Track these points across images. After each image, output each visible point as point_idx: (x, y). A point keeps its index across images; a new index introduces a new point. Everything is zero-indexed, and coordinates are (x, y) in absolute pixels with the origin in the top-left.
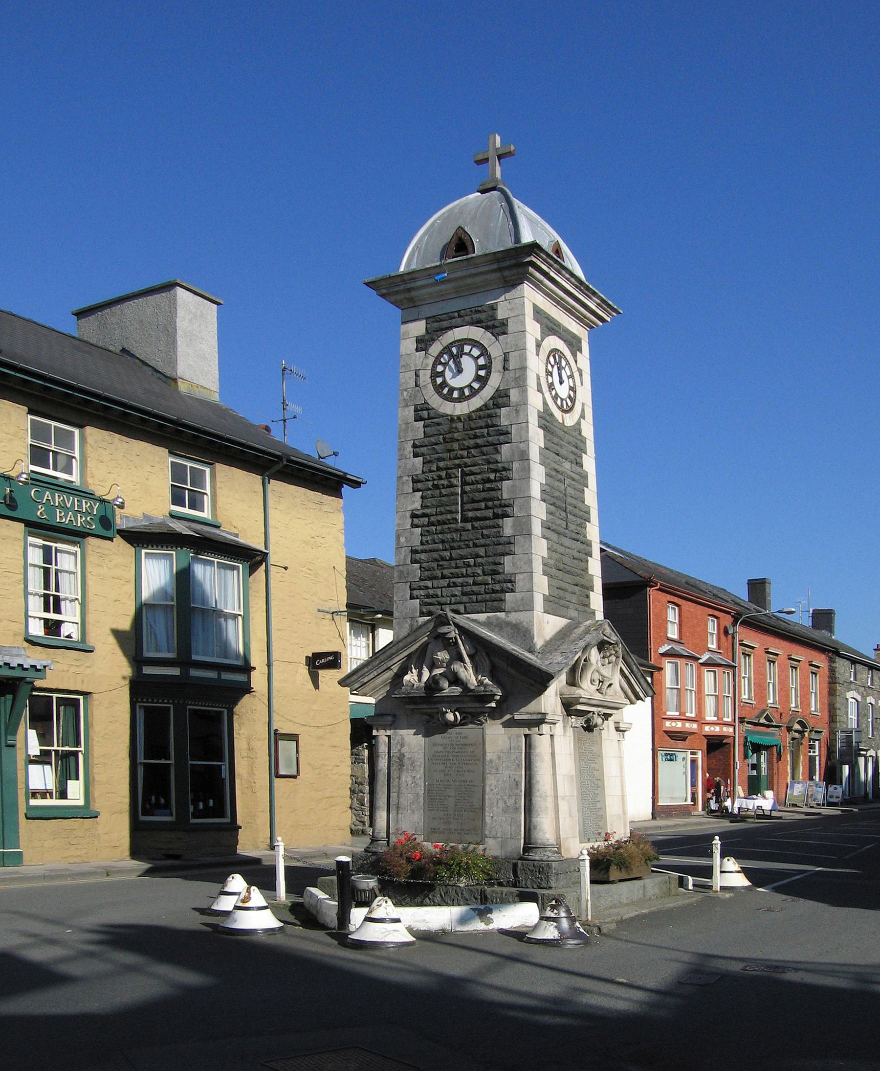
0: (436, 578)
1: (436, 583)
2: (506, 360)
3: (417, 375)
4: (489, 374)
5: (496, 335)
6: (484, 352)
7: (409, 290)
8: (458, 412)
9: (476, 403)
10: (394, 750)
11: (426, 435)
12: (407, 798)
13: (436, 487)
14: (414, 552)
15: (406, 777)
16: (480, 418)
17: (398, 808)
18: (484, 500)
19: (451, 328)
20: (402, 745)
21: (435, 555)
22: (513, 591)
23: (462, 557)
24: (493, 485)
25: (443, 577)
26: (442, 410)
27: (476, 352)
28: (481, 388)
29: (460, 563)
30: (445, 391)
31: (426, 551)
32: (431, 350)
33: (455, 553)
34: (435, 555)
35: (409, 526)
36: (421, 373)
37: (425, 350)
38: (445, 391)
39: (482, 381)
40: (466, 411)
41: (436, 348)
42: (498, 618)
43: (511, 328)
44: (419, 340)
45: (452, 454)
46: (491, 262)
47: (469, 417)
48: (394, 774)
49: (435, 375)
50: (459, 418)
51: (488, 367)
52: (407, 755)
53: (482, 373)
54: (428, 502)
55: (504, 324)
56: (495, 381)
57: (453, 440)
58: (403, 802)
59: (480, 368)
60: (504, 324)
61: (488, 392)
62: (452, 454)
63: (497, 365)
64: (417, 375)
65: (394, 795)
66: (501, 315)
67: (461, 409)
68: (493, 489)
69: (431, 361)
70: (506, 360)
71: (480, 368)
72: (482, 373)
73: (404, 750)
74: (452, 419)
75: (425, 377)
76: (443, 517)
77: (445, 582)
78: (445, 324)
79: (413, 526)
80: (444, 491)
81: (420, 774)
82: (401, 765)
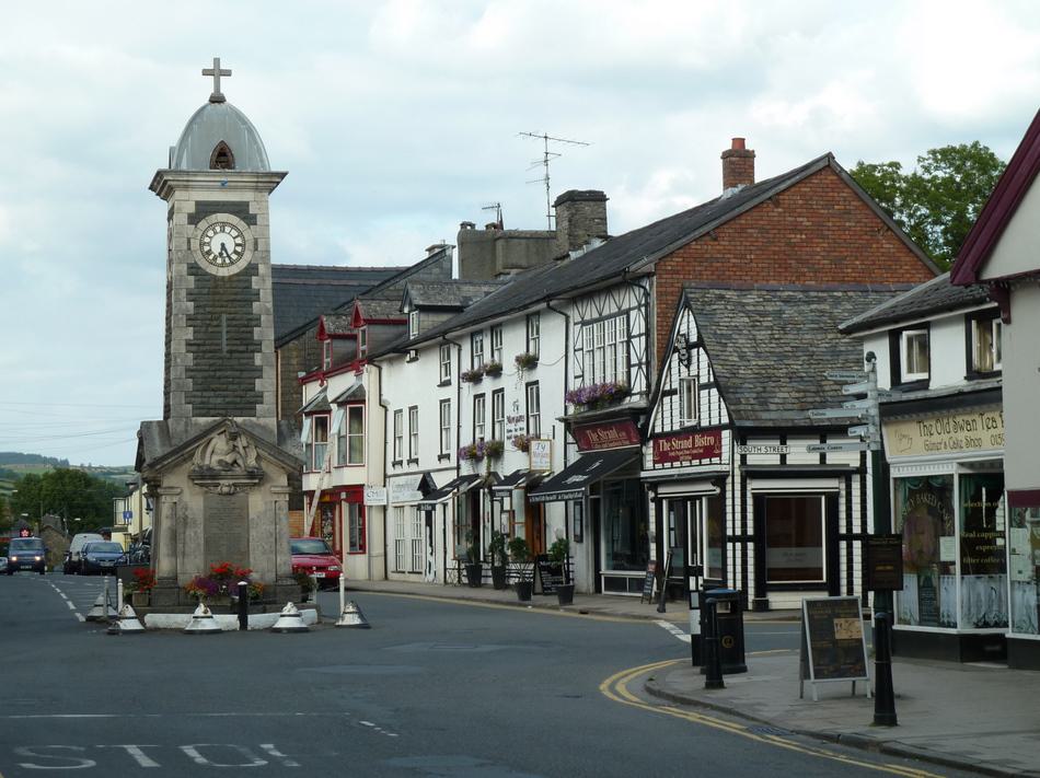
0: (205, 390)
1: (205, 394)
2: (256, 244)
3: (189, 242)
4: (244, 250)
6: (241, 234)
7: (188, 181)
8: (220, 274)
9: (234, 270)
10: (180, 513)
12: (191, 546)
15: (190, 532)
16: (239, 281)
17: (184, 554)
19: (215, 212)
20: (186, 509)
21: (206, 374)
22: (262, 403)
23: (227, 377)
24: (249, 329)
26: (208, 270)
27: (234, 233)
28: (238, 260)
29: (222, 380)
30: (211, 257)
32: (199, 225)
33: (218, 374)
34: (206, 374)
35: (184, 351)
36: (192, 241)
37: (196, 225)
38: (211, 257)
40: (227, 275)
41: (203, 225)
42: (251, 421)
47: (230, 277)
48: (180, 530)
49: (202, 244)
50: (223, 277)
52: (190, 517)
54: (199, 336)
55: (255, 216)
57: (218, 293)
59: (237, 245)
60: (255, 216)
61: (242, 264)
64: (189, 242)
65: (180, 546)
67: (223, 272)
69: (200, 233)
70: (256, 244)
71: (237, 245)
72: (239, 249)
74: (215, 277)
76: (213, 347)
77: (212, 394)
79: (188, 352)
81: (200, 530)
82: (185, 524)
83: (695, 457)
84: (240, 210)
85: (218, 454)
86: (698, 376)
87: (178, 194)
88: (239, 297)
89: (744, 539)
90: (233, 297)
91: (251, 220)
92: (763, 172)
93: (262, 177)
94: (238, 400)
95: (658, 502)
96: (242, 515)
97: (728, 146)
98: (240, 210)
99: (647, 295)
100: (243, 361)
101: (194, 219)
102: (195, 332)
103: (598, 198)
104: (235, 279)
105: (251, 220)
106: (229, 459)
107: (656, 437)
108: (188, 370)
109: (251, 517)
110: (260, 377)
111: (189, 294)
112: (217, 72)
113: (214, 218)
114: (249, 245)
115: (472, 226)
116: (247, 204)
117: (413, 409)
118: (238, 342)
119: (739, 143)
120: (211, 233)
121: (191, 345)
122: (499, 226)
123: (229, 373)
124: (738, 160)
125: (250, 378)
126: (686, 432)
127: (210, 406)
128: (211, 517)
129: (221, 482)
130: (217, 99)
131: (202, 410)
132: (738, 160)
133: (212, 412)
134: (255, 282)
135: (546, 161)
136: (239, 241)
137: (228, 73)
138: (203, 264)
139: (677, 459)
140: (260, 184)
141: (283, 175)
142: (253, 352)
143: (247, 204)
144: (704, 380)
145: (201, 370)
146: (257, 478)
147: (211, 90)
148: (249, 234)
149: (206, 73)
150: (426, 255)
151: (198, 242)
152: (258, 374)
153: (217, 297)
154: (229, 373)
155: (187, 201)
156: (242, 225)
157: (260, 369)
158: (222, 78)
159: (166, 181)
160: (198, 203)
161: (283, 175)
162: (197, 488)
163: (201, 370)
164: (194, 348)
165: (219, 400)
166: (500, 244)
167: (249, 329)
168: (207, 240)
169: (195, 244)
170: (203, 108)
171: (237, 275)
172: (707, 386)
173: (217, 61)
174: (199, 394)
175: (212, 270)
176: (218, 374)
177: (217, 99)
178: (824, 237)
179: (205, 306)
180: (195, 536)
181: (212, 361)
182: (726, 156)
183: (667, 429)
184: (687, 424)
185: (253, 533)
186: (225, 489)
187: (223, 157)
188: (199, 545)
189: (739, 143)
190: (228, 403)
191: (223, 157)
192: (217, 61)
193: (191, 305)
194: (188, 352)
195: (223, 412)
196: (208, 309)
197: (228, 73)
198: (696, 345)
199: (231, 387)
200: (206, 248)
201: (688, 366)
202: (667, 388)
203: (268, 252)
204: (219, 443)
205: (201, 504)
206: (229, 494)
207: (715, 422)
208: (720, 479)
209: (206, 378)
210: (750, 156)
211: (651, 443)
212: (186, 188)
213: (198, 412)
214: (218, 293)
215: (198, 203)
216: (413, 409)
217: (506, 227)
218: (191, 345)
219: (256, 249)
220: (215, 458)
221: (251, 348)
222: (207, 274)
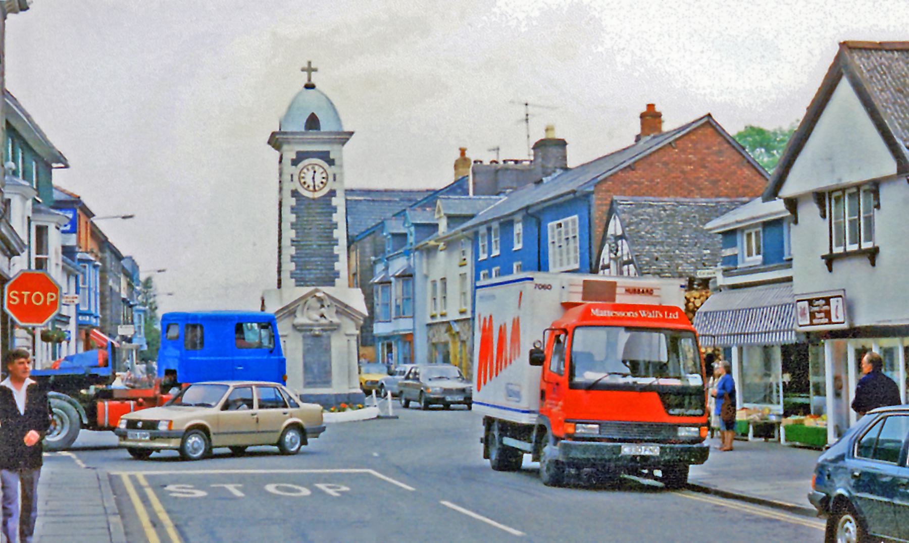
41: (301, 165)
43: (337, 162)
51: (327, 179)
53: (324, 181)
61: (325, 191)
66: (332, 156)
72: (324, 181)
87: (285, 147)
91: (331, 162)
97: (644, 109)
98: (325, 156)
101: (295, 163)
103: (562, 144)
105: (331, 162)
110: (337, 261)
112: (310, 69)
113: (306, 162)
114: (331, 178)
116: (328, 153)
117: (444, 280)
119: (651, 106)
120: (305, 170)
124: (651, 118)
130: (310, 86)
132: (651, 118)
134: (335, 201)
135: (527, 120)
136: (324, 175)
137: (315, 70)
141: (352, 133)
143: (328, 153)
144: (625, 258)
146: (334, 328)
147: (306, 81)
148: (331, 170)
149: (303, 70)
155: (290, 154)
156: (326, 165)
157: (337, 256)
158: (313, 73)
160: (298, 153)
161: (352, 133)
162: (297, 333)
168: (302, 175)
169: (296, 178)
170: (299, 94)
173: (310, 63)
177: (310, 86)
178: (705, 167)
182: (643, 116)
186: (317, 333)
189: (651, 106)
191: (313, 122)
192: (310, 63)
197: (315, 70)
200: (302, 181)
206: (317, 336)
210: (659, 115)
212: (289, 143)
215: (298, 153)
219: (335, 180)
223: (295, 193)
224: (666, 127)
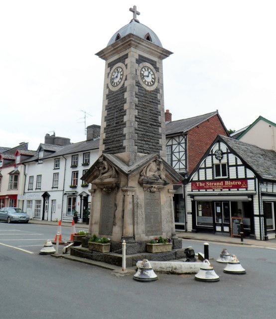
1: (143, 142)
2: (159, 80)
3: (136, 71)
5: (157, 71)
6: (154, 74)
7: (139, 43)
10: (135, 201)
11: (139, 92)
13: (143, 111)
14: (136, 129)
15: (139, 212)
16: (153, 94)
18: (155, 120)
21: (142, 133)
23: (150, 136)
24: (157, 116)
25: (145, 141)
28: (153, 85)
29: (149, 137)
31: (139, 130)
33: (147, 134)
34: (142, 133)
39: (154, 83)
40: (149, 90)
44: (137, 60)
45: (147, 102)
46: (161, 50)
48: (136, 210)
51: (155, 79)
56: (156, 84)
57: (146, 97)
58: (139, 221)
59: (153, 78)
62: (147, 102)
63: (157, 80)
64: (136, 71)
66: (158, 65)
67: (148, 88)
68: (157, 117)
69: (140, 69)
70: (159, 80)
73: (139, 201)
74: (145, 90)
75: (138, 73)
76: (145, 121)
77: (144, 142)
78: (144, 60)
80: (145, 113)
83: (224, 188)
84: (153, 63)
85: (152, 171)
86: (228, 163)
88: (154, 101)
89: (259, 216)
90: (151, 100)
91: (157, 69)
92: (174, 119)
93: (164, 52)
94: (154, 147)
95: (193, 202)
96: (159, 204)
98: (153, 63)
99: (186, 140)
100: (155, 130)
102: (138, 112)
104: (152, 92)
106: (156, 174)
107: (192, 181)
108: (136, 129)
109: (162, 204)
110: (161, 138)
111: (136, 94)
112: (133, 10)
114: (157, 80)
115: (48, 135)
117: (39, 176)
118: (154, 121)
121: (137, 118)
122: (54, 135)
123: (150, 134)
125: (158, 138)
126: (214, 181)
127: (145, 148)
128: (147, 204)
129: (154, 186)
131: (141, 150)
133: (146, 151)
136: (153, 76)
137: (138, 14)
138: (141, 82)
139: (211, 188)
140: (162, 56)
141: (172, 53)
142: (158, 126)
143: (156, 62)
145: (140, 131)
149: (131, 10)
150: (19, 145)
151: (139, 72)
152: (160, 136)
153: (146, 99)
154: (150, 134)
159: (132, 40)
160: (140, 56)
161: (172, 53)
163: (140, 131)
164: (138, 120)
165: (147, 146)
166: (56, 140)
167: (157, 116)
169: (138, 73)
171: (153, 91)
172: (236, 166)
173: (135, 7)
174: (139, 141)
175: (144, 86)
176: (147, 134)
179: (142, 101)
180: (141, 213)
181: (145, 127)
183: (202, 178)
184: (216, 178)
185: (163, 212)
187: (148, 38)
188: (143, 218)
190: (150, 148)
192: (135, 7)
193: (137, 99)
194: (136, 121)
195: (149, 152)
196: (144, 103)
197: (138, 14)
198: (227, 153)
199: (151, 141)
201: (220, 160)
202: (203, 166)
203: (163, 84)
204: (153, 166)
205: (143, 196)
207: (241, 175)
208: (251, 196)
209: (142, 134)
210: (171, 114)
211: (190, 183)
212: (136, 47)
213: (139, 150)
214: (146, 97)
215: (140, 56)
216: (39, 176)
217: (56, 136)
218: (137, 118)
220: (152, 173)
221: (159, 124)
222: (142, 87)
223: (138, 84)
224: (173, 120)
